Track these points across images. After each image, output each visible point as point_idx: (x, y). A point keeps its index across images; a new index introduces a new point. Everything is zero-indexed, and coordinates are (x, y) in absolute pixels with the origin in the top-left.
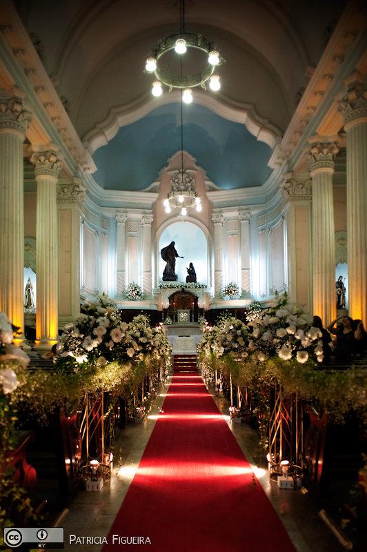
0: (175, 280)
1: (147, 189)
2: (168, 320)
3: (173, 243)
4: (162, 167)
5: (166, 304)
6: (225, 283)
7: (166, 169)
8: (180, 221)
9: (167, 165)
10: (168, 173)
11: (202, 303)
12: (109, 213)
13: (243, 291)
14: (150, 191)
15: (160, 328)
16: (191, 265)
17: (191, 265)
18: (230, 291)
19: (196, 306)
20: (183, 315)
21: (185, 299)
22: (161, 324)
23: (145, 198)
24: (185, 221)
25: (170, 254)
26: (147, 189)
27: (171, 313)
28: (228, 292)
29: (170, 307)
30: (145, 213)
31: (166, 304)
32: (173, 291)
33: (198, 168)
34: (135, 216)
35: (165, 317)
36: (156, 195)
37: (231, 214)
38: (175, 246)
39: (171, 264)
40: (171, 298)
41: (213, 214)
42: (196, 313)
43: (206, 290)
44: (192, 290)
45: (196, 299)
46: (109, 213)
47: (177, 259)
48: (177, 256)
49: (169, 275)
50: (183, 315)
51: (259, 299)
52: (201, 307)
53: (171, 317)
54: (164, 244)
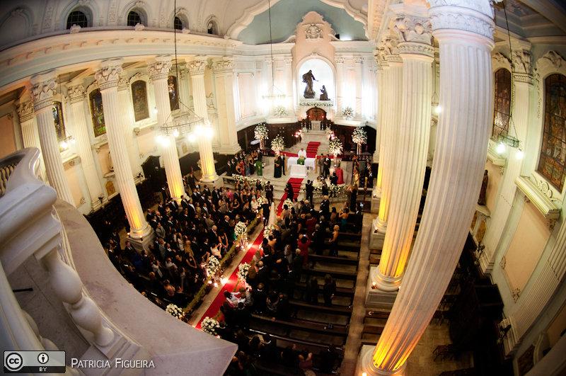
0: (312, 97)
1: (288, 40)
2: (305, 129)
4: (298, 23)
6: (344, 107)
7: (302, 23)
9: (302, 21)
10: (302, 28)
11: (329, 117)
12: (260, 58)
13: (356, 114)
14: (289, 42)
15: (299, 134)
17: (324, 87)
18: (347, 113)
19: (325, 118)
20: (316, 123)
21: (317, 113)
23: (286, 46)
26: (288, 40)
27: (306, 123)
28: (345, 114)
30: (285, 56)
31: (305, 116)
32: (309, 108)
33: (324, 22)
34: (280, 57)
36: (293, 44)
37: (350, 56)
39: (310, 85)
40: (308, 112)
42: (326, 124)
43: (332, 108)
44: (323, 107)
45: (325, 113)
46: (260, 58)
50: (316, 123)
51: (368, 119)
52: (328, 119)
54: (304, 71)
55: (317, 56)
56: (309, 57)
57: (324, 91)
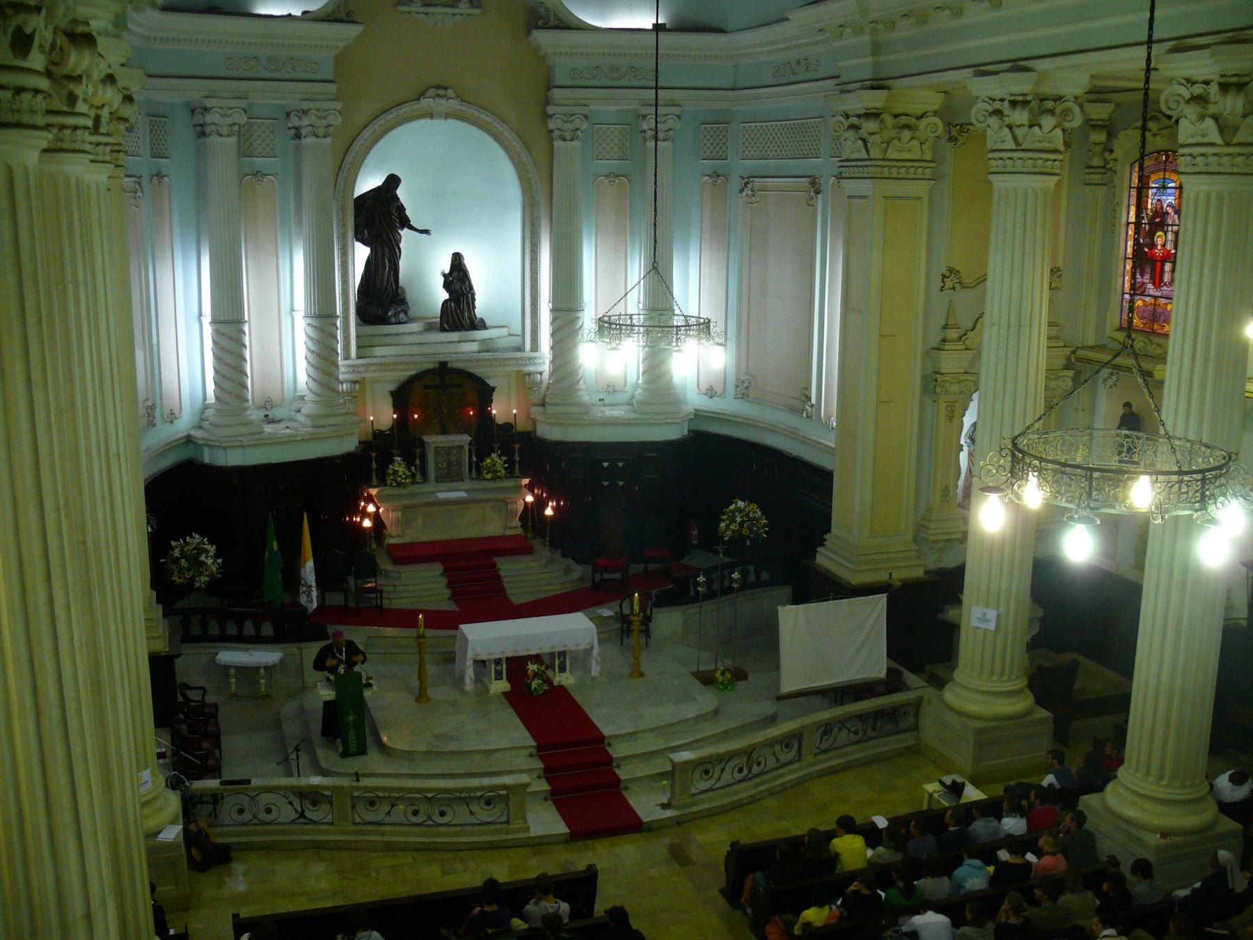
3: (393, 182)
5: (383, 415)
8: (431, 116)
16: (457, 260)
17: (457, 260)
19: (485, 417)
22: (374, 492)
24: (447, 116)
25: (381, 218)
29: (401, 424)
35: (387, 460)
36: (349, 32)
38: (400, 192)
40: (401, 397)
41: (550, 110)
45: (485, 393)
47: (405, 233)
48: (406, 223)
49: (382, 298)
53: (409, 463)
55: (454, 104)
56: (406, 109)
57: (457, 278)
